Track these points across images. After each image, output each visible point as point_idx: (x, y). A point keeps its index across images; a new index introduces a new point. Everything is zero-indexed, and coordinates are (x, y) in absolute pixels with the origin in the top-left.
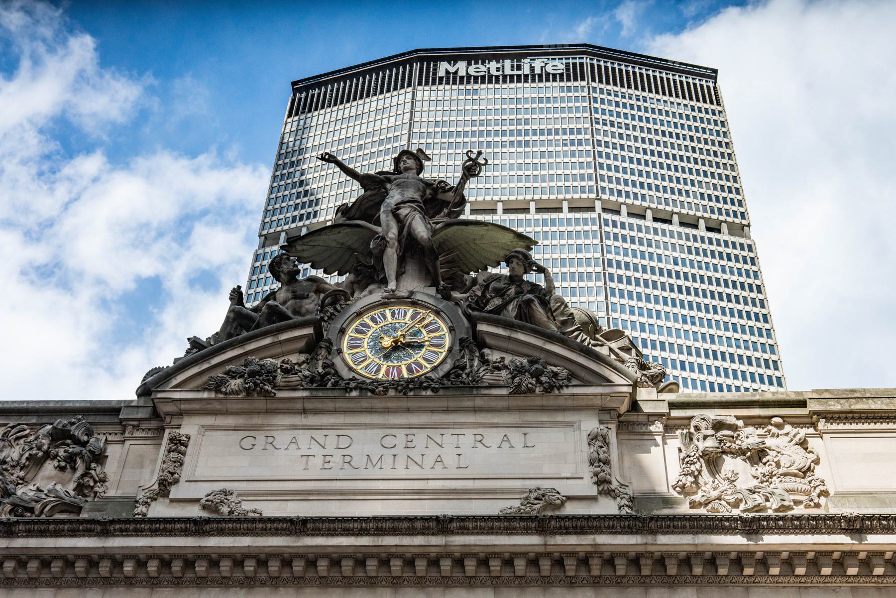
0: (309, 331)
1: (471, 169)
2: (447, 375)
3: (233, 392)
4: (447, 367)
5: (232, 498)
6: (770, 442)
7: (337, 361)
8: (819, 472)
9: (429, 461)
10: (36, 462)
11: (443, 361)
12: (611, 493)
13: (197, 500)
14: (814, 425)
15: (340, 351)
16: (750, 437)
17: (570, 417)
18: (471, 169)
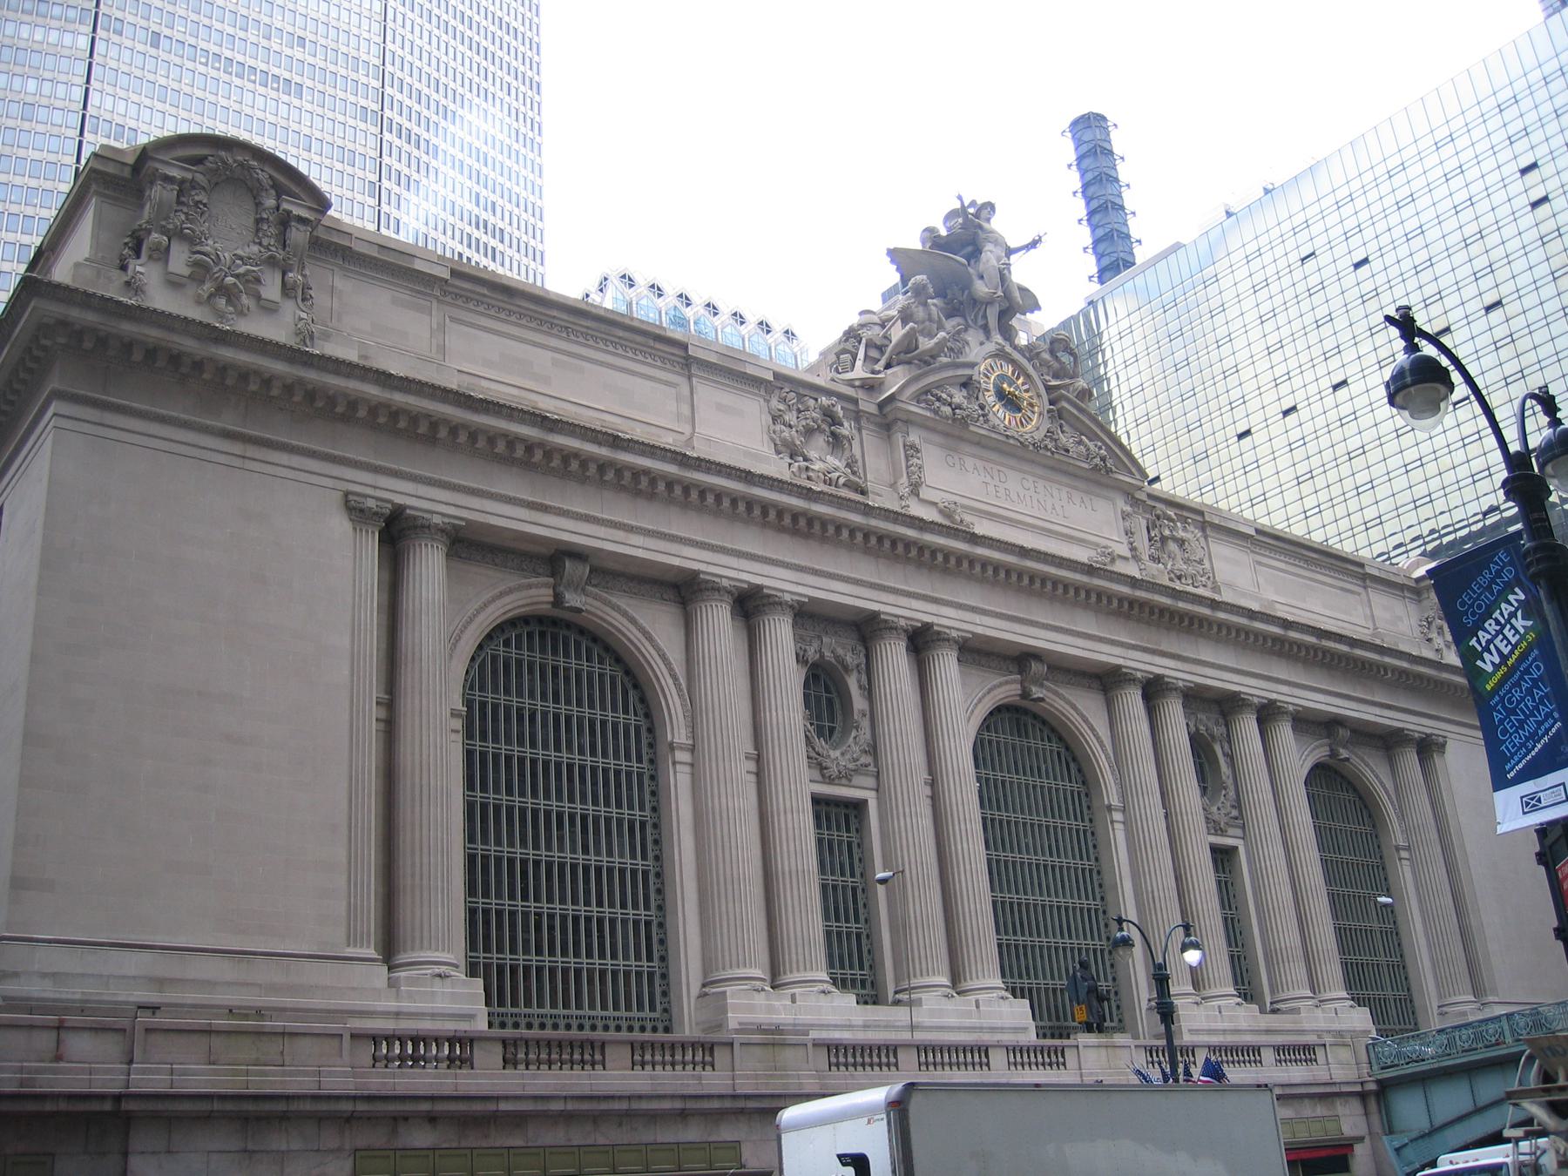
1: (1034, 244)
3: (947, 418)
4: (1043, 432)
8: (1207, 565)
9: (1049, 508)
10: (809, 432)
12: (1136, 558)
13: (935, 504)
14: (1203, 530)
17: (1112, 494)
18: (1034, 244)
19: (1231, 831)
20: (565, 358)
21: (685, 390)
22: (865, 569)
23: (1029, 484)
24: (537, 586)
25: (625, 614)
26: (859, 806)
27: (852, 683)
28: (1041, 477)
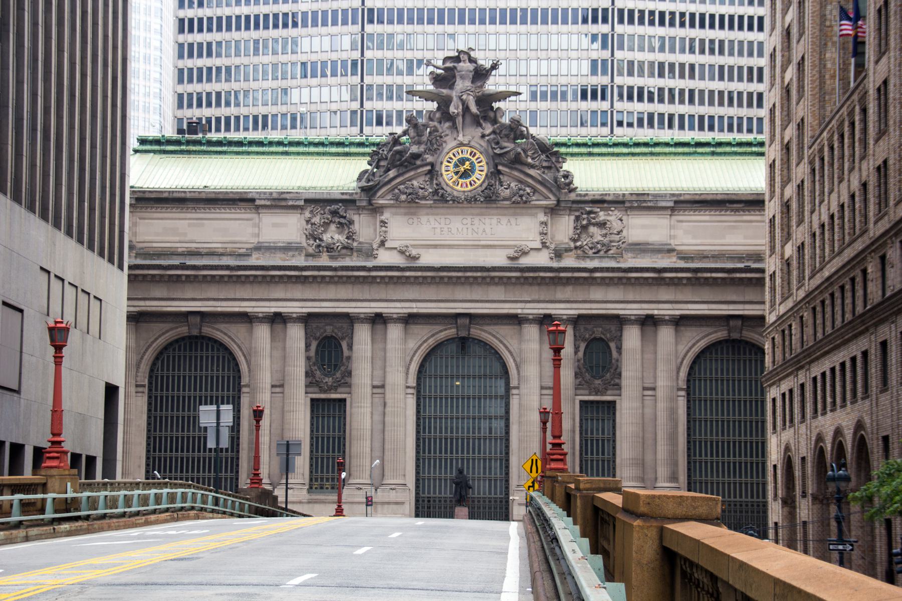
0: (429, 168)
1: (494, 67)
2: (486, 189)
4: (485, 185)
5: (410, 249)
6: (609, 218)
7: (441, 180)
8: (624, 233)
9: (480, 231)
10: (326, 225)
11: (484, 182)
12: (548, 248)
14: (626, 211)
15: (442, 175)
16: (602, 216)
17: (534, 211)
19: (609, 392)
20: (195, 221)
21: (257, 221)
22: (344, 292)
23: (468, 220)
24: (180, 327)
25: (222, 332)
26: (344, 400)
27: (344, 345)
28: (478, 215)
